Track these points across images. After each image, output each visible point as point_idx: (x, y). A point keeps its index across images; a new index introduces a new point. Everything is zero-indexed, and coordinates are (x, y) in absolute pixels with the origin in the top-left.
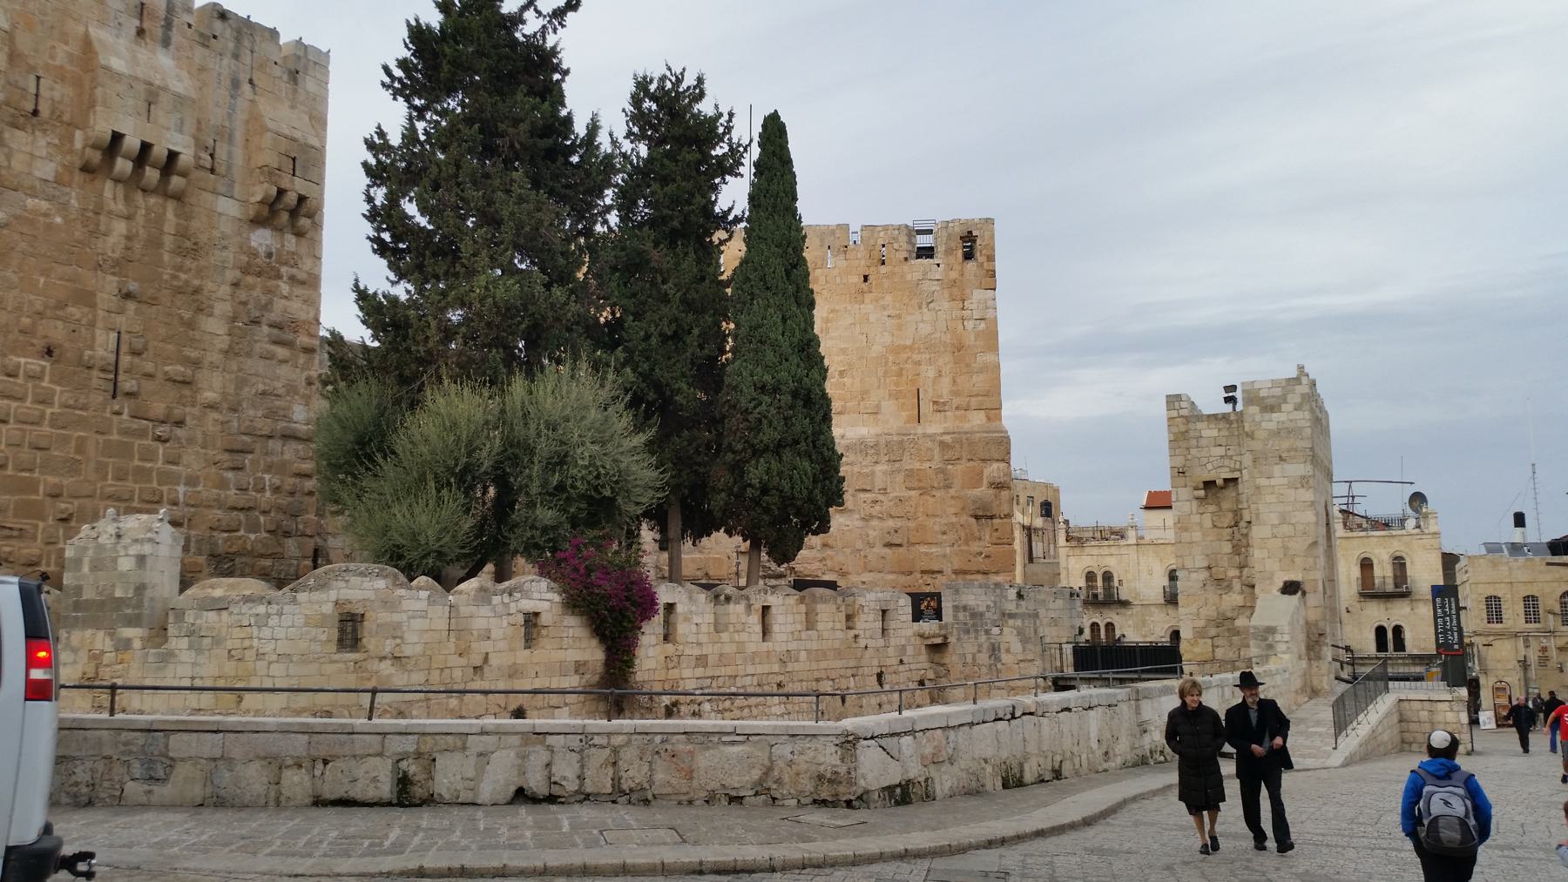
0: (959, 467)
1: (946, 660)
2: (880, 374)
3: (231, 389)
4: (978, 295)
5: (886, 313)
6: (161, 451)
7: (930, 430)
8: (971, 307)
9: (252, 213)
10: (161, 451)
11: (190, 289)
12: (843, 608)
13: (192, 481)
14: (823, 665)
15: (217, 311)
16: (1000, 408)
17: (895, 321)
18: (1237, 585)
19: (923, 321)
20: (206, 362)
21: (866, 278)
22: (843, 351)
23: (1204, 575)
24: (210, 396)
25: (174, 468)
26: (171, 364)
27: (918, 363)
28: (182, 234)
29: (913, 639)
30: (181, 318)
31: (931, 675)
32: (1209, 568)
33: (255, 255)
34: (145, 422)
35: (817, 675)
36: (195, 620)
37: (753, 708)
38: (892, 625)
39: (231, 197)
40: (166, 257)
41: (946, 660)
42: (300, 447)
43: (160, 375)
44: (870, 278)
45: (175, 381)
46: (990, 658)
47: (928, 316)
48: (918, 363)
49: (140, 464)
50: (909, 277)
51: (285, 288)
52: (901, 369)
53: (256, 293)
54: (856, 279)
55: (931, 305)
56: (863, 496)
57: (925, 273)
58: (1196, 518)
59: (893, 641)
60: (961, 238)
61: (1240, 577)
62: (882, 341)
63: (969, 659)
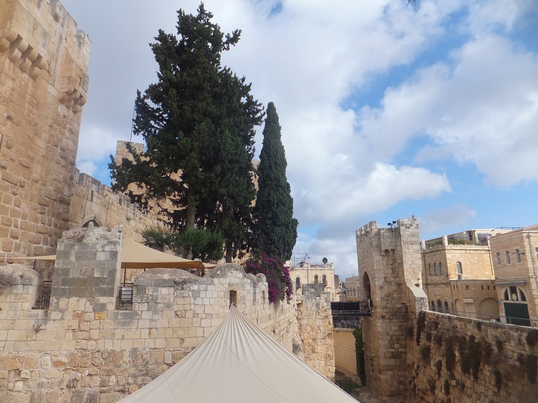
3: (44, 175)
6: (13, 199)
9: (61, 96)
10: (13, 199)
11: (34, 123)
13: (24, 217)
15: (42, 137)
18: (394, 283)
20: (36, 160)
23: (383, 280)
24: (36, 176)
25: (18, 209)
26: (22, 157)
28: (33, 96)
30: (29, 136)
32: (385, 278)
33: (59, 116)
34: (8, 183)
36: (153, 293)
39: (54, 86)
40: (26, 105)
42: (66, 207)
43: (17, 161)
45: (23, 166)
49: (4, 204)
51: (67, 134)
53: (57, 132)
58: (381, 261)
61: (394, 281)
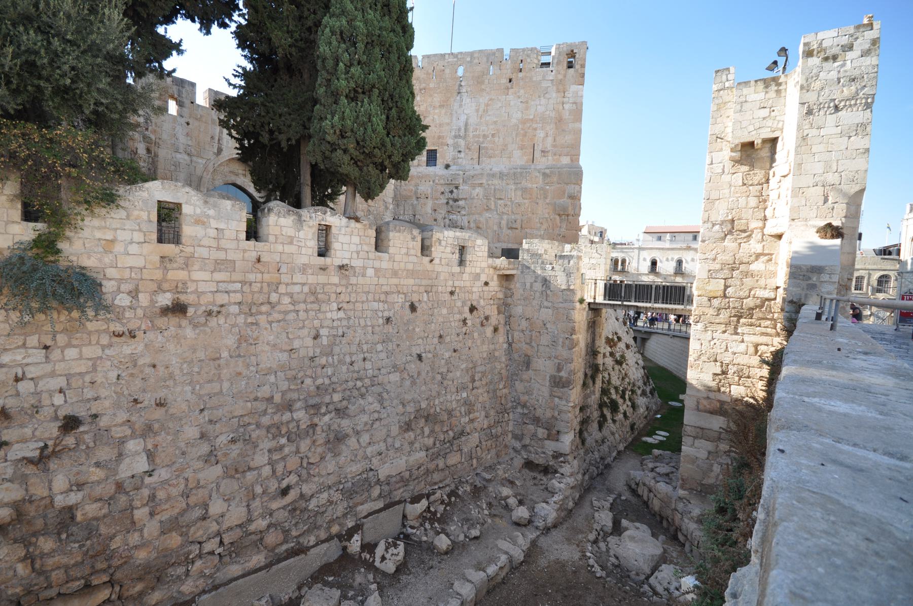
0: (552, 188)
1: (512, 286)
2: (514, 135)
4: (574, 88)
5: (520, 100)
7: (538, 167)
8: (569, 96)
12: (419, 239)
14: (394, 281)
16: (579, 155)
17: (524, 105)
19: (540, 105)
21: (510, 81)
22: (495, 123)
27: (535, 129)
29: (487, 270)
31: (501, 295)
35: (385, 288)
37: (301, 313)
38: (468, 257)
41: (512, 286)
44: (513, 80)
46: (543, 286)
47: (543, 101)
48: (535, 129)
50: (534, 79)
52: (526, 132)
54: (505, 81)
55: (546, 95)
56: (500, 202)
57: (544, 76)
59: (468, 269)
60: (567, 55)
62: (517, 116)
63: (528, 285)
